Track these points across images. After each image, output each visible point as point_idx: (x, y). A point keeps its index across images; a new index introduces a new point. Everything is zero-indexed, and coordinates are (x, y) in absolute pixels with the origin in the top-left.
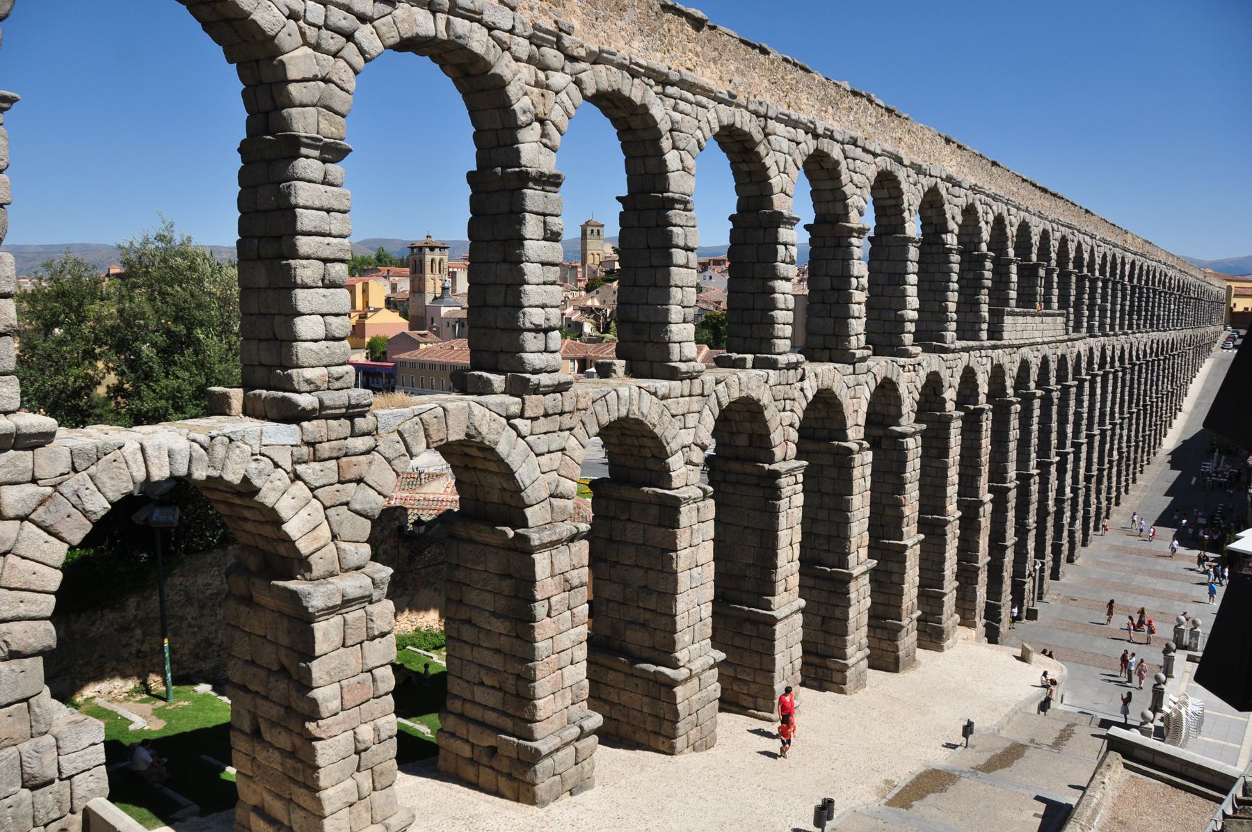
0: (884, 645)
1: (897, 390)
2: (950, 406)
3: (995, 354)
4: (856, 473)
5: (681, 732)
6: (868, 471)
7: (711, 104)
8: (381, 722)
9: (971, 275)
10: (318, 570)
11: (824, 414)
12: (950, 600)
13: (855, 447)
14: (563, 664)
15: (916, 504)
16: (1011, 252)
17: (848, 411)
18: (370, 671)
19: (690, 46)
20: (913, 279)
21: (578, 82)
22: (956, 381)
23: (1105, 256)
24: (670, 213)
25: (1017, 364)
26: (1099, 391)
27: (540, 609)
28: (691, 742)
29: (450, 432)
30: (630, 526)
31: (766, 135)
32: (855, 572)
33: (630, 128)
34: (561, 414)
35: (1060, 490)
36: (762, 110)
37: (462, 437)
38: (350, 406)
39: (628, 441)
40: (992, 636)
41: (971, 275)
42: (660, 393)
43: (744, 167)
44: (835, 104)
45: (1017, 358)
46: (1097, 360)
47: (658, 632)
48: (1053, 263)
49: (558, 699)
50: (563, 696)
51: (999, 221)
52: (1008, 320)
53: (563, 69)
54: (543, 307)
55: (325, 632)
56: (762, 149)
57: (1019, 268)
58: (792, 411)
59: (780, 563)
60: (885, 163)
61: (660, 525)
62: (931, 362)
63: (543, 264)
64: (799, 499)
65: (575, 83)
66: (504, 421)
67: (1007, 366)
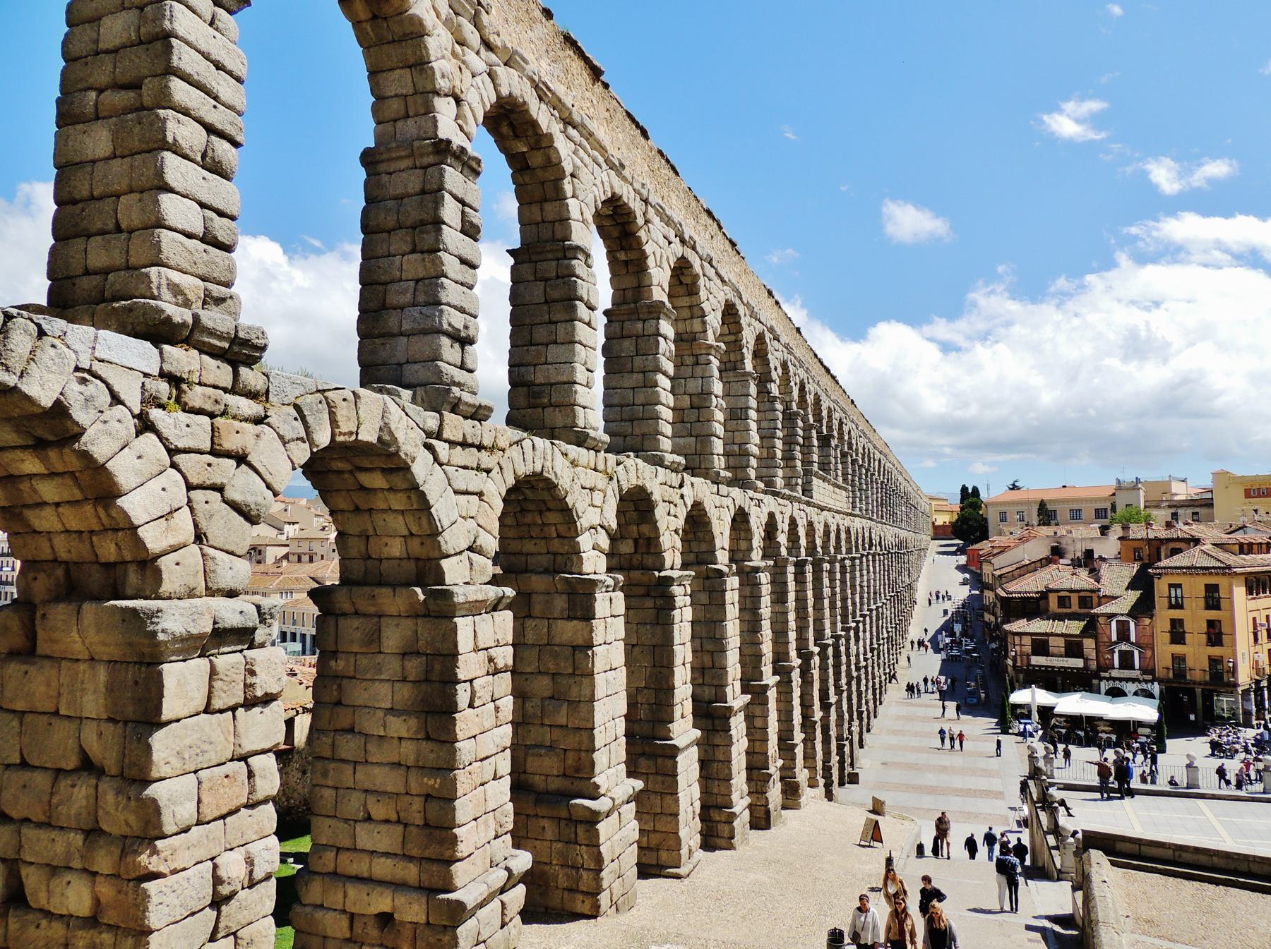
1: (748, 522)
2: (784, 552)
3: (808, 509)
5: (605, 884)
7: (605, 166)
8: (254, 848)
10: (174, 574)
13: (725, 569)
18: (244, 758)
19: (588, 94)
21: (492, 75)
22: (786, 528)
24: (574, 262)
31: (647, 222)
33: (528, 167)
34: (480, 447)
36: (644, 192)
37: (373, 439)
38: (235, 340)
39: (528, 519)
40: (829, 796)
42: (571, 457)
43: (622, 256)
44: (696, 218)
46: (867, 540)
47: (570, 755)
49: (482, 827)
50: (486, 823)
52: (815, 481)
53: (478, 53)
54: (462, 310)
55: (182, 682)
60: (731, 295)
61: (570, 618)
62: (770, 503)
64: (688, 613)
65: (489, 75)
67: (816, 525)
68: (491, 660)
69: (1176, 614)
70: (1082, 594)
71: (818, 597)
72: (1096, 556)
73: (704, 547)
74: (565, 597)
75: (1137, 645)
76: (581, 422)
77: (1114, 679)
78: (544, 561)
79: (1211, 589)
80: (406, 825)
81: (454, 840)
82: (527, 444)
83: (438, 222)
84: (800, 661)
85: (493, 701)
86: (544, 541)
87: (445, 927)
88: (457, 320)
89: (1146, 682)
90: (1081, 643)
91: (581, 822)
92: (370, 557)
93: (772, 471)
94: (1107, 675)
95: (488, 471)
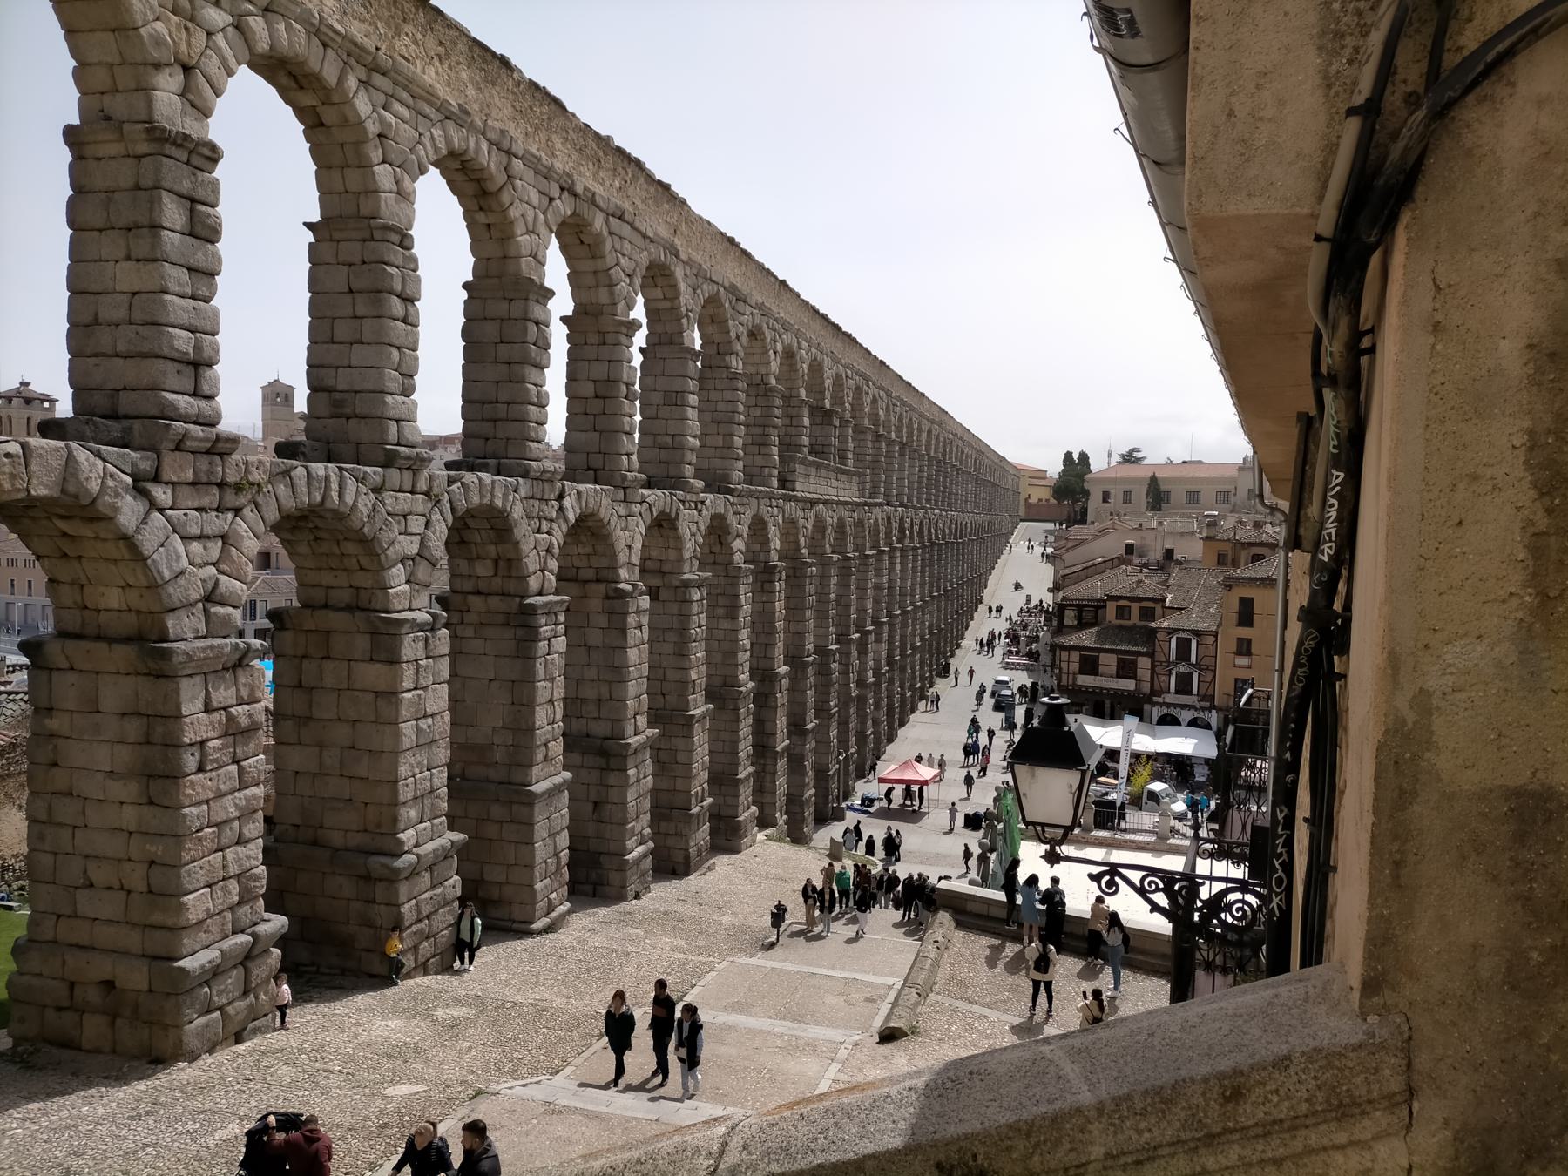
0: (671, 842)
1: (676, 529)
4: (632, 620)
6: (645, 620)
9: (758, 412)
11: (588, 549)
12: (745, 793)
13: (628, 587)
14: (224, 841)
15: (703, 668)
16: (803, 392)
17: (620, 545)
20: (693, 399)
22: (745, 530)
23: (900, 420)
25: (811, 521)
26: (898, 567)
27: (191, 762)
28: (421, 960)
29: (35, 481)
30: (328, 665)
32: (633, 741)
33: (322, 125)
35: (862, 671)
36: (505, 145)
41: (758, 412)
43: (482, 218)
45: (811, 514)
48: (848, 415)
50: (225, 889)
51: (789, 354)
56: (505, 198)
57: (812, 408)
58: (548, 533)
59: (538, 723)
62: (715, 503)
63: (189, 269)
64: (561, 643)
66: (129, 480)
67: (802, 521)
68: (231, 719)
69: (1245, 632)
70: (1145, 604)
71: (795, 610)
72: (1177, 556)
73: (604, 563)
74: (368, 637)
75: (1198, 666)
77: (1169, 705)
78: (345, 596)
80: (129, 892)
81: (182, 908)
82: (299, 472)
83: (156, 227)
84: (751, 685)
85: (235, 761)
87: (168, 994)
88: (183, 341)
89: (1203, 709)
90: (1134, 663)
93: (728, 464)
94: (1160, 700)
95: (237, 511)
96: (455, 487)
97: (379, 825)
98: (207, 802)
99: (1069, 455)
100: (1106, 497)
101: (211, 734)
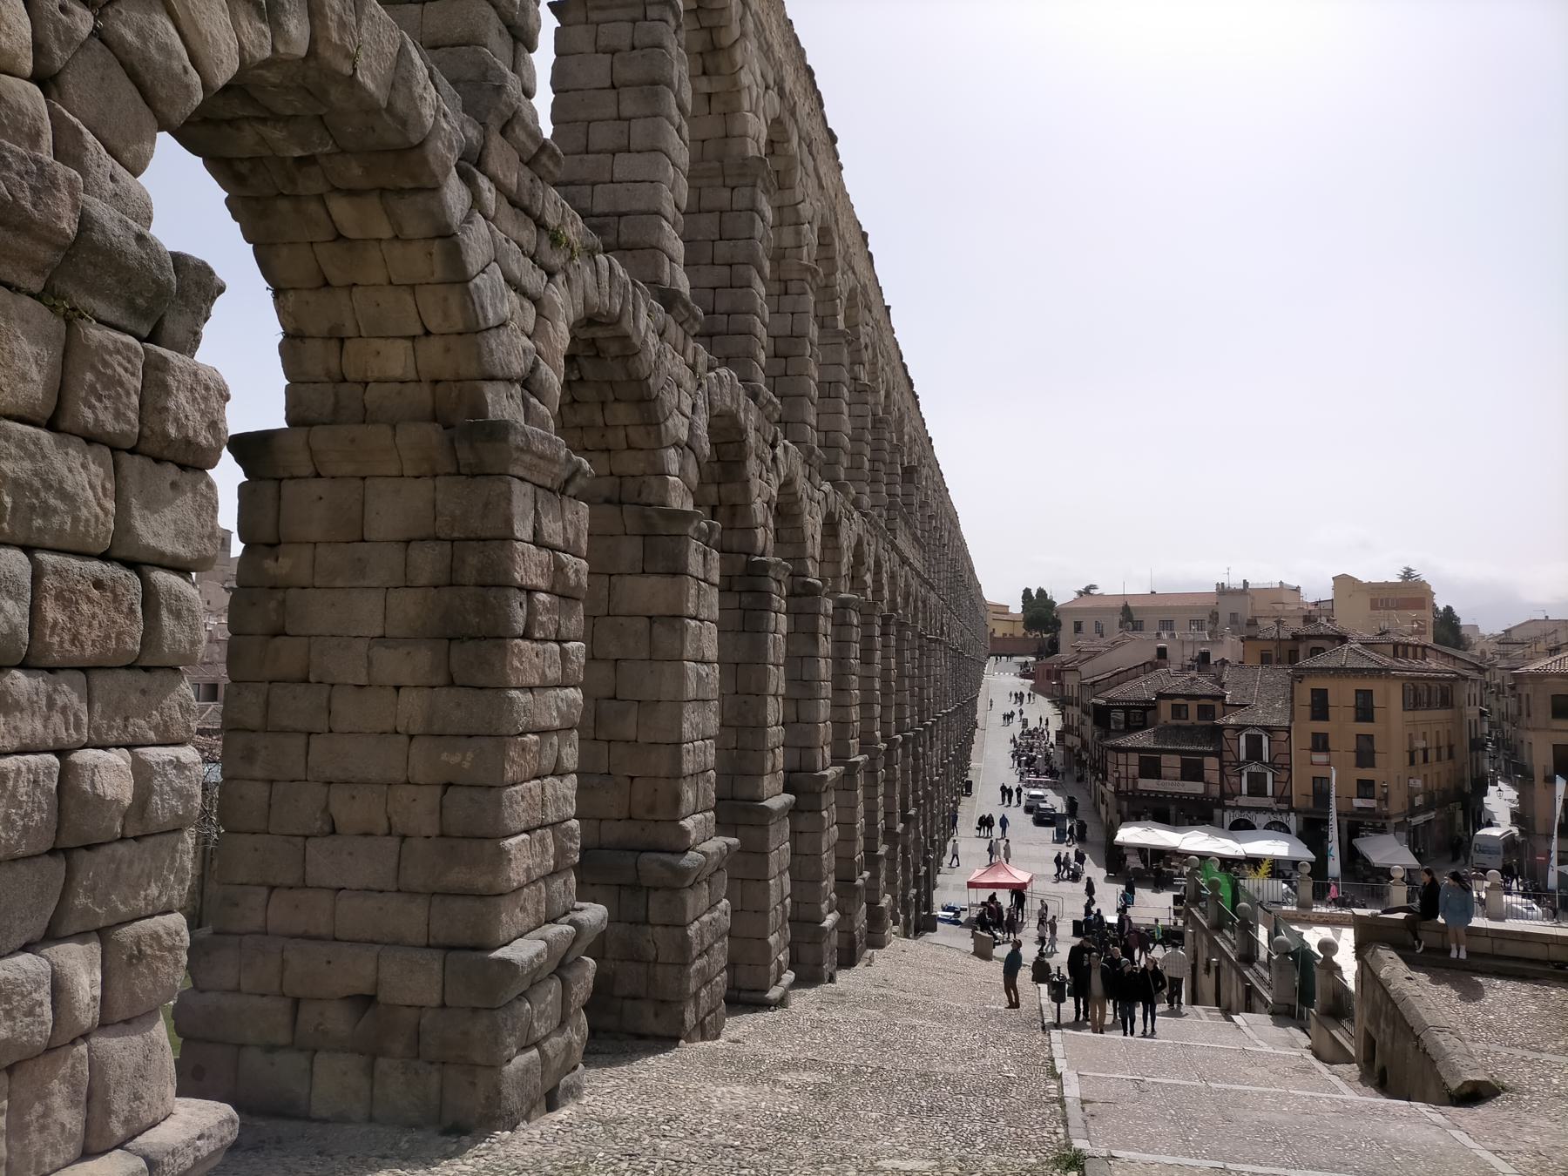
68: (560, 567)
69: (1320, 726)
74: (639, 540)
75: (1271, 764)
76: (666, 278)
77: (1242, 809)
79: (1365, 697)
80: (404, 837)
86: (605, 455)
87: (475, 1010)
89: (1280, 812)
90: (1202, 762)
91: (656, 889)
92: (344, 380)
95: (551, 275)
96: (712, 374)
97: (651, 809)
98: (531, 689)
99: (1027, 592)
100: (1078, 627)
101: (542, 583)
